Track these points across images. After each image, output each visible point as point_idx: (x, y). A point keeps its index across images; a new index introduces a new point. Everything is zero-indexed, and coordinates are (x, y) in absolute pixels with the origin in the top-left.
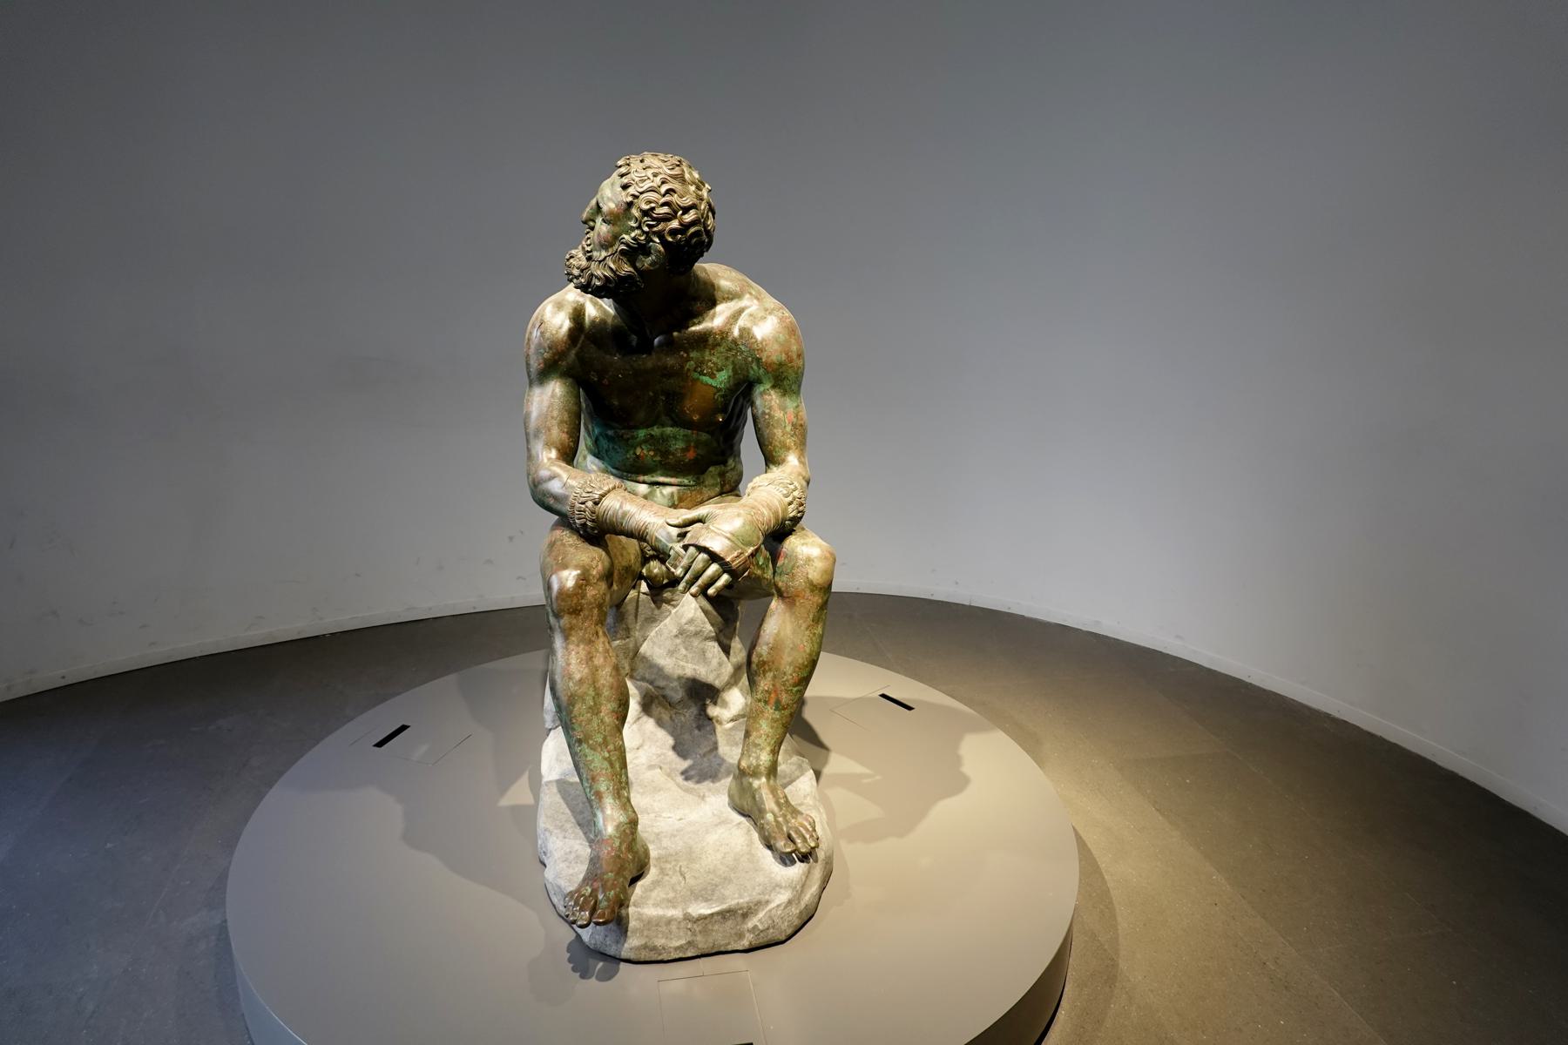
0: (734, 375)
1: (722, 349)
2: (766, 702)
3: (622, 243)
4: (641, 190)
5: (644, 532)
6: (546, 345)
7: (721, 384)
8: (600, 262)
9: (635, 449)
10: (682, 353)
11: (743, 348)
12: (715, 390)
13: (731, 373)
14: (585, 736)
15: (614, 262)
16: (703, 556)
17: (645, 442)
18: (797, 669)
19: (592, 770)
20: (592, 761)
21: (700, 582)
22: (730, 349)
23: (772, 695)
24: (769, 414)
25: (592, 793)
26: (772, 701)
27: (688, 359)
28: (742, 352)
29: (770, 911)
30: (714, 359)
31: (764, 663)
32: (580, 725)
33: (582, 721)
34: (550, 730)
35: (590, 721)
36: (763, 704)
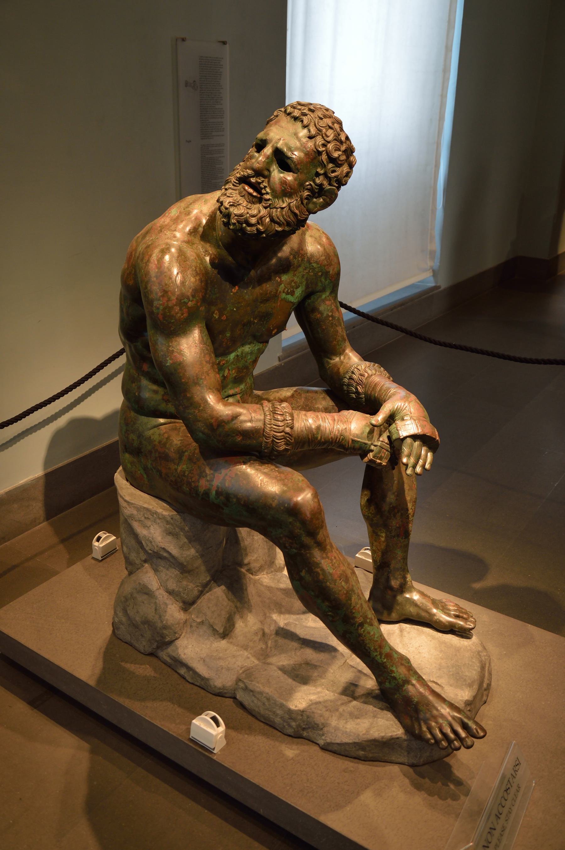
0: (306, 289)
1: (301, 269)
2: (398, 536)
3: (307, 189)
5: (339, 439)
6: (189, 294)
7: (296, 299)
8: (282, 208)
9: (225, 371)
10: (277, 278)
11: (315, 265)
12: (292, 304)
13: (304, 288)
15: (297, 207)
16: (417, 444)
18: (414, 503)
19: (377, 641)
20: (374, 635)
21: (421, 462)
22: (305, 269)
23: (401, 529)
24: (332, 316)
25: (383, 657)
27: (280, 283)
28: (314, 269)
30: (295, 279)
31: (394, 508)
32: (359, 612)
33: (359, 608)
35: (362, 604)
36: (396, 538)
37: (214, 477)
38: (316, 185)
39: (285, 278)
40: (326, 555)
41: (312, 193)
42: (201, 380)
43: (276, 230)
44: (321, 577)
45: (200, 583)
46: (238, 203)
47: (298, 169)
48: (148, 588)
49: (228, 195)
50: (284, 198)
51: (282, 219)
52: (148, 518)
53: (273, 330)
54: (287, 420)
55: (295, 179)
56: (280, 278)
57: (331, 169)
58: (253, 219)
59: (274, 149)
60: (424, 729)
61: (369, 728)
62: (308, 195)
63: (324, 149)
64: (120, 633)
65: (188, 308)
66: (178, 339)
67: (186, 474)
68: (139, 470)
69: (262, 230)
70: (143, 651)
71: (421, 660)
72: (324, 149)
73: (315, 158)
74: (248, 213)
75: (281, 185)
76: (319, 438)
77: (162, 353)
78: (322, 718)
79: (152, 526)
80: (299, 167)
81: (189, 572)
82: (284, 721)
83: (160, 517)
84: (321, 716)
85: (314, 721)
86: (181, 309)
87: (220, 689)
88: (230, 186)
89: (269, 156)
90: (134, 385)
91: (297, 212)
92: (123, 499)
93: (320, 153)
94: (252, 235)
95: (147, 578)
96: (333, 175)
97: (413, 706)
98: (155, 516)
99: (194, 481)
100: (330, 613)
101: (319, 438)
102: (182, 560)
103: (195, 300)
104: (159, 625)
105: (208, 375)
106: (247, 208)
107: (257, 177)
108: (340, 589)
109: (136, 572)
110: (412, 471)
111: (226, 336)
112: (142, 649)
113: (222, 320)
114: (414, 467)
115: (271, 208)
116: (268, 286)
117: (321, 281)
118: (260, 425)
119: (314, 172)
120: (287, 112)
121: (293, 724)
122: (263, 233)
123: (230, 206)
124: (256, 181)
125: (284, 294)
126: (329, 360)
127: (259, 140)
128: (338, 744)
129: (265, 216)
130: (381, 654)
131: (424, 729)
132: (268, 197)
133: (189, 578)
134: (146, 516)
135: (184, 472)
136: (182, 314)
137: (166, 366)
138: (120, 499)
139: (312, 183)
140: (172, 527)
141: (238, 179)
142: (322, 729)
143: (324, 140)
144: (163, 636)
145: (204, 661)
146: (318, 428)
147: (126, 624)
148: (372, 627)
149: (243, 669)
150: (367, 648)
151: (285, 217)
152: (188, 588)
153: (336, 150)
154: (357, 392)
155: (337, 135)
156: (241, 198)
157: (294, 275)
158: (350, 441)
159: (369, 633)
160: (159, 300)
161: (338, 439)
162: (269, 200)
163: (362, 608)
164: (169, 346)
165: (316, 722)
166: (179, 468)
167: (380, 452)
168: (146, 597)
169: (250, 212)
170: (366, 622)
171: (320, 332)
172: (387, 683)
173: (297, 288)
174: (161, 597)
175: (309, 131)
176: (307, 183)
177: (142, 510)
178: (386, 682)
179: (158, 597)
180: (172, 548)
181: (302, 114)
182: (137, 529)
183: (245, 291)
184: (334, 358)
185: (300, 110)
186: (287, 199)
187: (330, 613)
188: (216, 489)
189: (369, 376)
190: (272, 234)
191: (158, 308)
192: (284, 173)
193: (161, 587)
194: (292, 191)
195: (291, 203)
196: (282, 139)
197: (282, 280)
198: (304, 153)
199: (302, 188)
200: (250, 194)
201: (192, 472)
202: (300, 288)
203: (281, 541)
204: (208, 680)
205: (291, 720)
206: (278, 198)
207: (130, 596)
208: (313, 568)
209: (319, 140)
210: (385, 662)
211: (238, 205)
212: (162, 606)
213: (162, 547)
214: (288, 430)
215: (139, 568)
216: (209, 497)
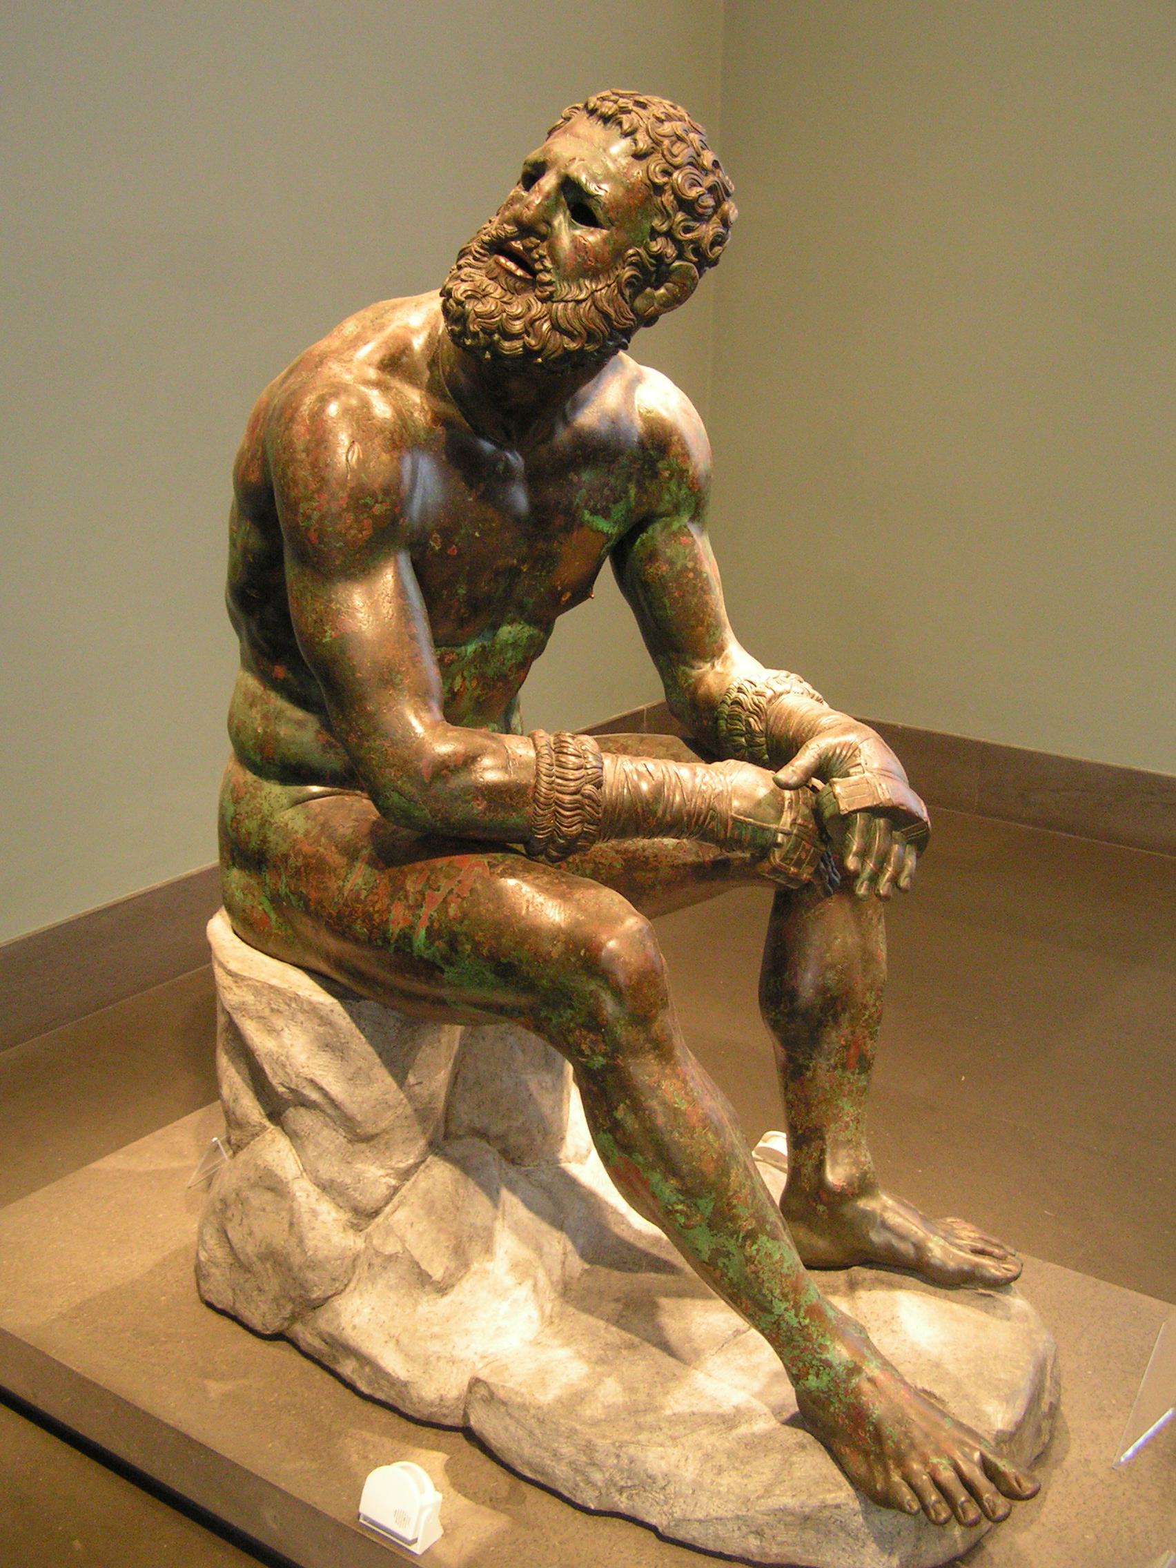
2: (845, 1067)
3: (631, 264)
4: (678, 161)
8: (579, 302)
9: (454, 680)
14: (758, 1221)
17: (472, 661)
19: (788, 1276)
20: (782, 1259)
21: (889, 872)
23: (852, 1051)
24: (694, 570)
25: (802, 1313)
26: (853, 1061)
29: (1052, 1372)
31: (834, 1000)
34: (329, 1297)
37: (424, 899)
38: (651, 257)
39: (586, 476)
40: (673, 1070)
41: (640, 271)
42: (399, 676)
43: (565, 349)
44: (661, 1120)
45: (392, 1169)
47: (610, 220)
48: (276, 1175)
49: (463, 277)
50: (581, 281)
52: (278, 1010)
53: (562, 594)
54: (586, 769)
55: (605, 241)
57: (682, 224)
58: (517, 322)
60: (896, 1478)
61: (771, 1485)
62: (632, 276)
63: (666, 179)
64: (211, 1287)
65: (374, 517)
66: (349, 587)
67: (362, 897)
68: (261, 904)
69: (536, 348)
70: (259, 1328)
71: (895, 1346)
72: (666, 179)
73: (648, 199)
76: (660, 813)
77: (314, 617)
78: (663, 1463)
79: (286, 1029)
80: (611, 214)
81: (368, 1139)
82: (576, 1471)
83: (306, 1007)
84: (662, 1458)
85: (645, 1471)
86: (357, 520)
87: (431, 1404)
90: (254, 710)
91: (611, 311)
92: (225, 968)
93: (658, 189)
94: (514, 358)
95: (274, 1153)
96: (689, 236)
97: (871, 1428)
98: (294, 1005)
99: (378, 912)
100: (680, 1207)
101: (660, 813)
102: (352, 1108)
103: (388, 500)
104: (297, 1260)
105: (414, 666)
108: (703, 1148)
109: (248, 1143)
110: (868, 889)
111: (458, 594)
112: (257, 1323)
113: (449, 556)
114: (874, 879)
115: (553, 302)
117: (669, 489)
118: (525, 778)
119: (646, 226)
120: (590, 108)
121: (597, 1477)
122: (538, 353)
123: (466, 298)
125: (586, 512)
126: (687, 670)
128: (700, 1521)
129: (540, 319)
130: (797, 1306)
131: (896, 1478)
132: (547, 277)
133: (369, 1154)
134: (273, 1006)
135: (358, 894)
136: (360, 532)
137: (324, 645)
138: (218, 971)
139: (641, 251)
140: (331, 1032)
141: (486, 246)
142: (664, 1488)
143: (668, 162)
144: (303, 1286)
145: (398, 1341)
146: (658, 790)
147: (223, 1265)
148: (776, 1244)
149: (486, 1360)
150: (765, 1291)
151: (584, 320)
152: (364, 1178)
153: (692, 185)
154: (750, 732)
155: (695, 155)
156: (491, 282)
157: (610, 472)
158: (730, 823)
159: (769, 1255)
160: (311, 499)
161: (702, 817)
162: (550, 283)
163: (755, 1197)
164: (331, 601)
165: (650, 1471)
166: (348, 886)
167: (795, 848)
168: (269, 1196)
169: (507, 308)
170: (764, 1231)
171: (668, 605)
172: (810, 1377)
173: (616, 502)
174: (304, 1195)
175: (635, 141)
176: (631, 252)
177: (266, 992)
178: (808, 1374)
179: (298, 1194)
180: (330, 1079)
182: (252, 1035)
184: (701, 664)
186: (587, 283)
187: (680, 1207)
188: (428, 924)
189: (777, 696)
190: (556, 358)
191: (309, 518)
193: (304, 1174)
194: (599, 265)
195: (597, 291)
197: (583, 479)
200: (510, 273)
201: (375, 891)
202: (622, 503)
203: (571, 1039)
204: (406, 1384)
205: (593, 1469)
206: (568, 280)
207: (234, 1196)
208: (643, 1099)
209: (655, 165)
210: (806, 1326)
212: (306, 1218)
213: (309, 1077)
214: (589, 789)
215: (257, 1135)
216: (411, 946)
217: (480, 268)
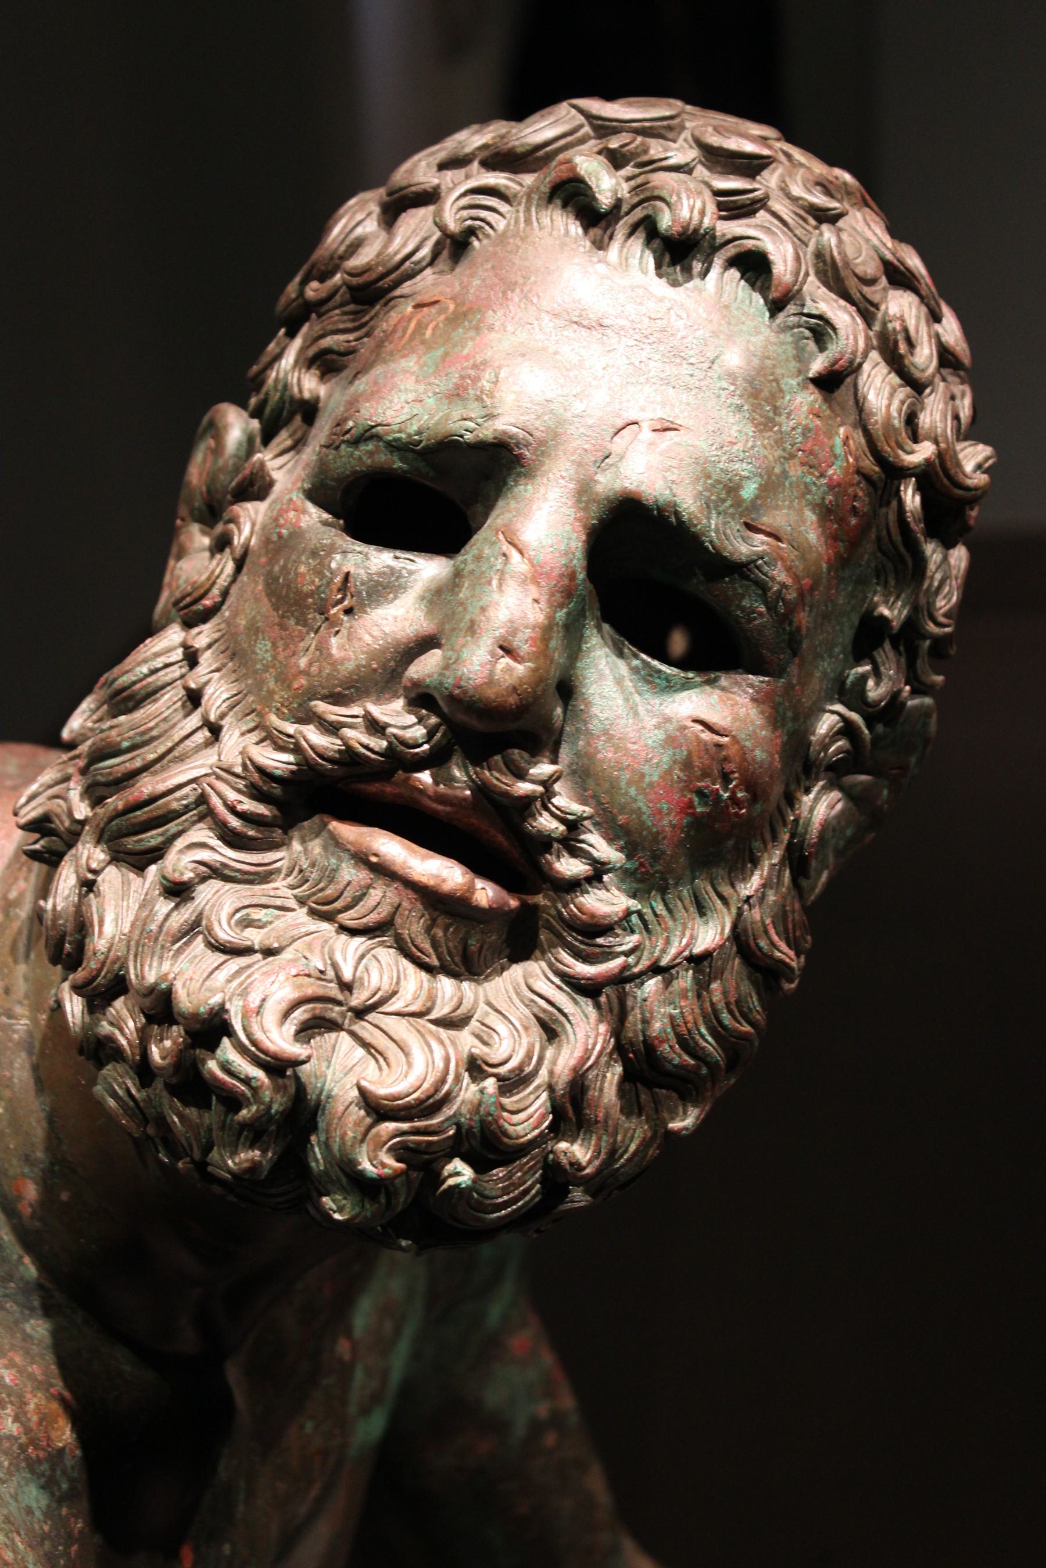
46: (357, 999)
49: (225, 933)
51: (708, 1043)
56: (348, 1333)
59: (595, 512)
69: (588, 1171)
74: (476, 1068)
75: (687, 785)
88: (204, 855)
89: (572, 576)
106: (436, 1022)
107: (477, 756)
116: (309, 1426)
124: (482, 790)
127: (397, 447)
176: (825, 724)
181: (720, 206)
183: (227, 1549)
185: (684, 169)
192: (686, 686)
196: (645, 426)
198: (815, 506)
199: (800, 769)
206: (663, 891)
211: (360, 1013)
217: (264, 877)
